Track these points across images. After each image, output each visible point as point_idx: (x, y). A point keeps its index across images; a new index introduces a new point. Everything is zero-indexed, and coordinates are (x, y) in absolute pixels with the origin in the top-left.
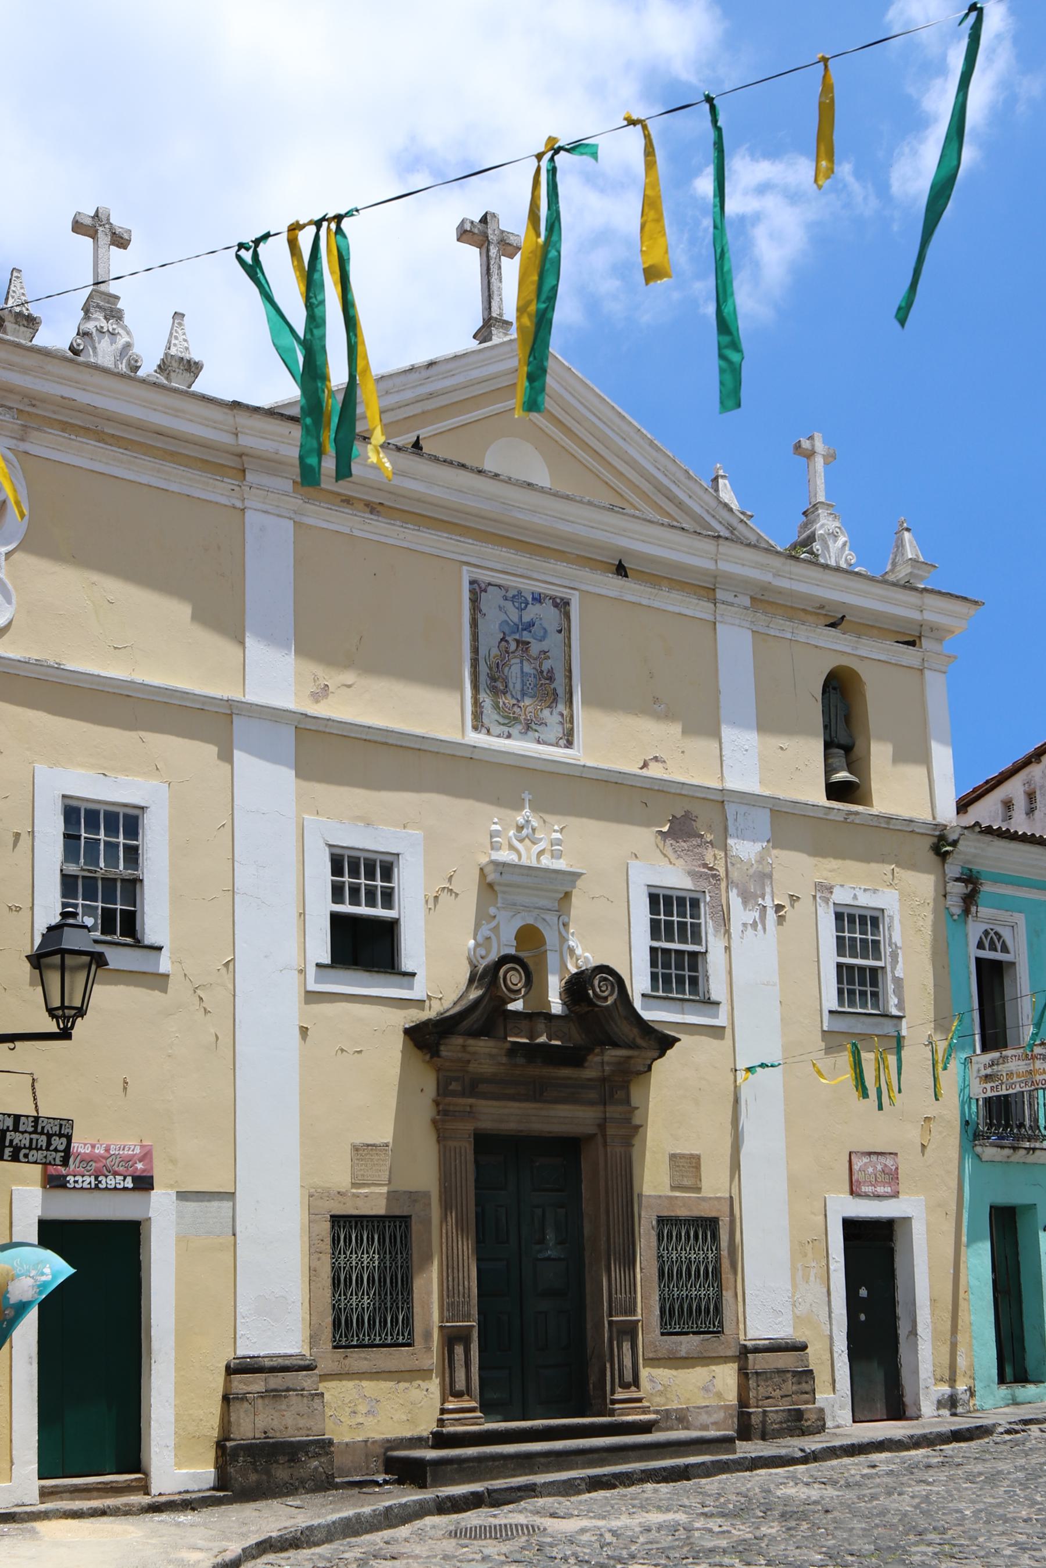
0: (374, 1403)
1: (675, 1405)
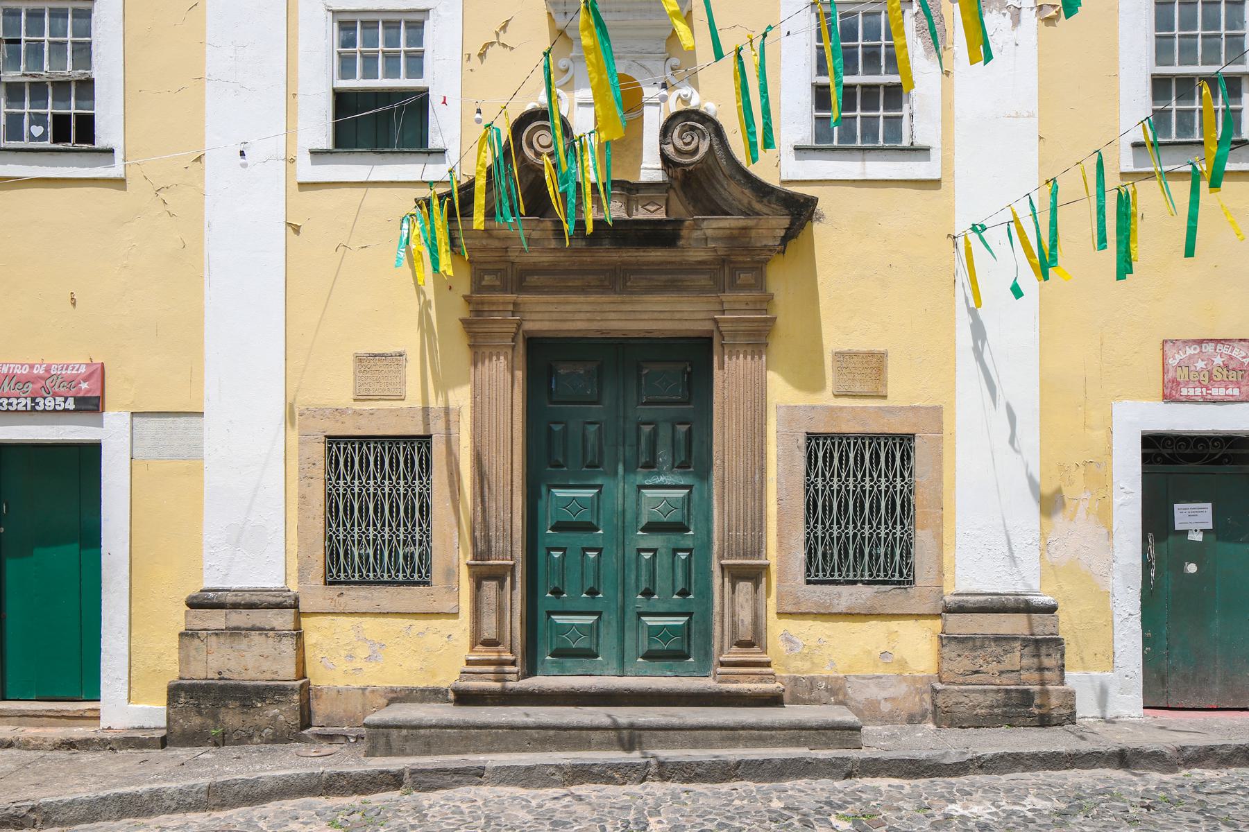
0: (377, 647)
1: (826, 672)
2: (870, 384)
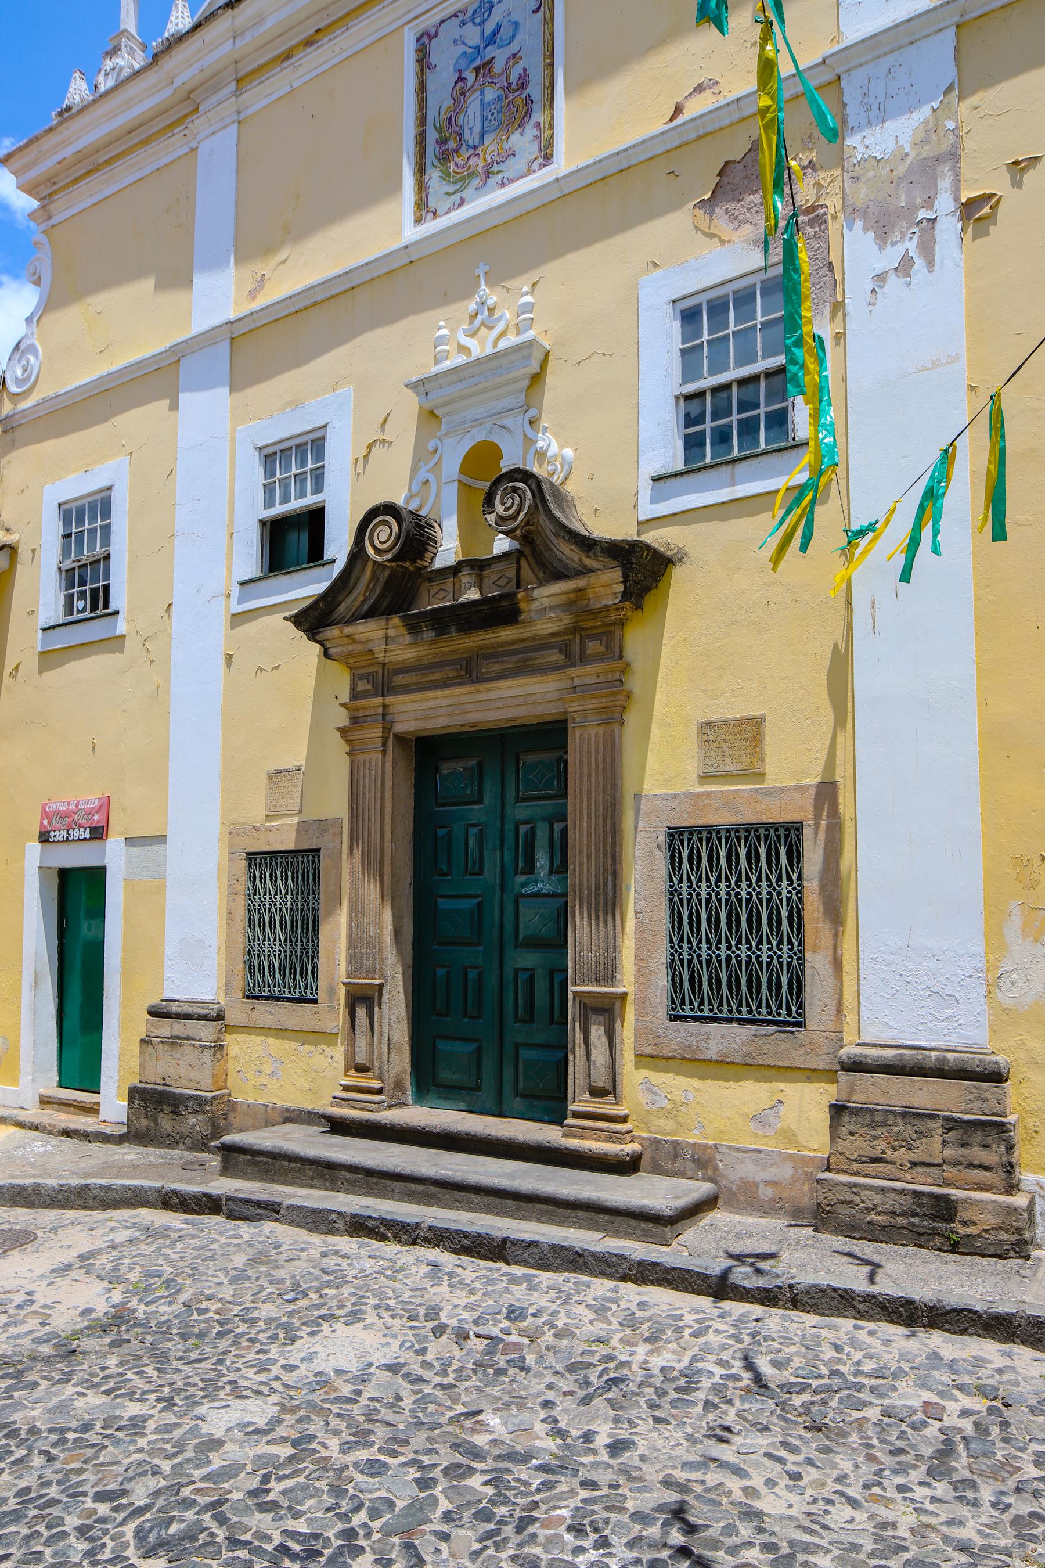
2: (744, 759)
